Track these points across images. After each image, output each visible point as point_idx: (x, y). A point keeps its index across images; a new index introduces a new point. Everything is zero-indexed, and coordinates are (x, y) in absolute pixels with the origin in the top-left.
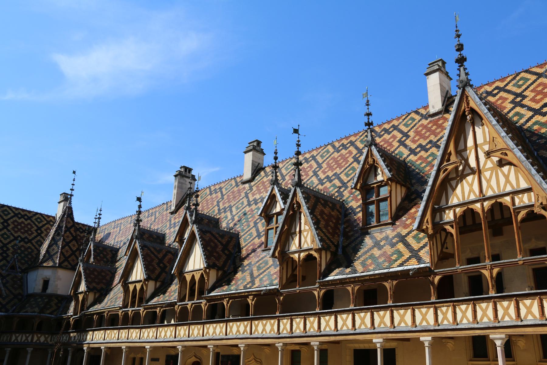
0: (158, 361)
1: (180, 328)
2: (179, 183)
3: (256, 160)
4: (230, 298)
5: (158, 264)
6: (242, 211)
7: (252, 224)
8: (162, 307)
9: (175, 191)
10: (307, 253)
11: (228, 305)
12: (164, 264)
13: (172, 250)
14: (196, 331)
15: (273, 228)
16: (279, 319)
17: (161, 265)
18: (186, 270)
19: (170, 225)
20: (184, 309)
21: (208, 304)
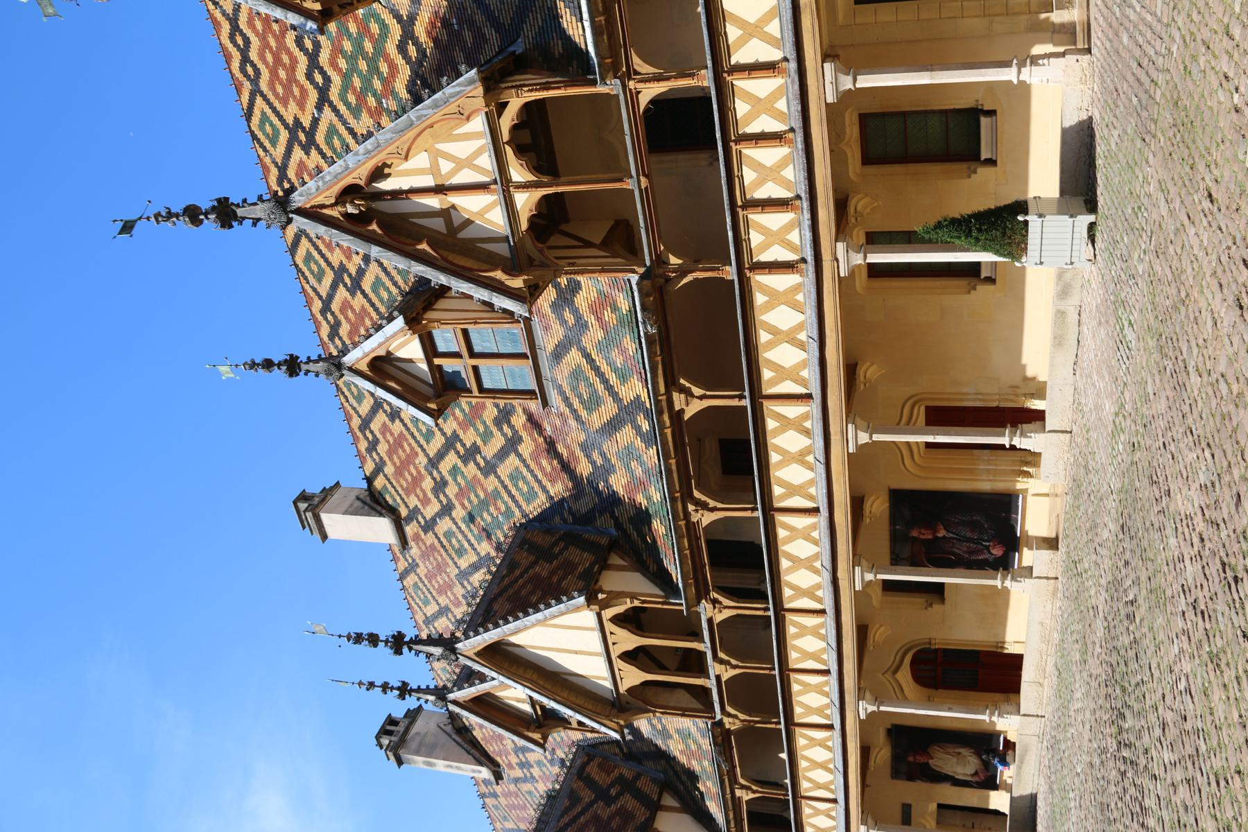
0: (910, 806)
1: (798, 710)
2: (417, 752)
3: (347, 503)
4: (688, 496)
5: (609, 801)
6: (463, 527)
7: (491, 483)
8: (733, 781)
9: (440, 765)
10: (509, 149)
11: (712, 503)
12: (612, 785)
13: (579, 762)
14: (808, 642)
15: (476, 369)
16: (748, 266)
17: (613, 792)
18: (608, 684)
19: (525, 780)
20: (738, 692)
21: (714, 595)
